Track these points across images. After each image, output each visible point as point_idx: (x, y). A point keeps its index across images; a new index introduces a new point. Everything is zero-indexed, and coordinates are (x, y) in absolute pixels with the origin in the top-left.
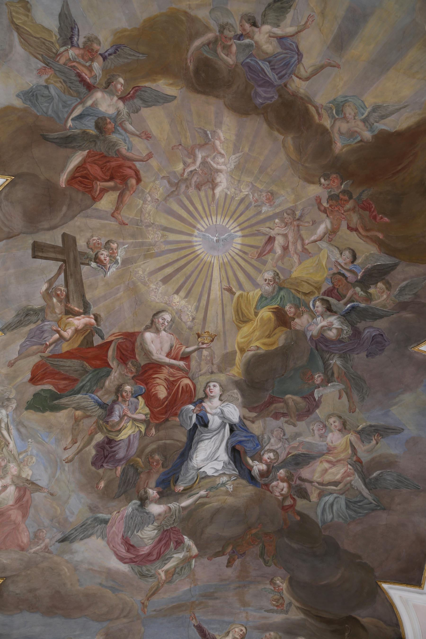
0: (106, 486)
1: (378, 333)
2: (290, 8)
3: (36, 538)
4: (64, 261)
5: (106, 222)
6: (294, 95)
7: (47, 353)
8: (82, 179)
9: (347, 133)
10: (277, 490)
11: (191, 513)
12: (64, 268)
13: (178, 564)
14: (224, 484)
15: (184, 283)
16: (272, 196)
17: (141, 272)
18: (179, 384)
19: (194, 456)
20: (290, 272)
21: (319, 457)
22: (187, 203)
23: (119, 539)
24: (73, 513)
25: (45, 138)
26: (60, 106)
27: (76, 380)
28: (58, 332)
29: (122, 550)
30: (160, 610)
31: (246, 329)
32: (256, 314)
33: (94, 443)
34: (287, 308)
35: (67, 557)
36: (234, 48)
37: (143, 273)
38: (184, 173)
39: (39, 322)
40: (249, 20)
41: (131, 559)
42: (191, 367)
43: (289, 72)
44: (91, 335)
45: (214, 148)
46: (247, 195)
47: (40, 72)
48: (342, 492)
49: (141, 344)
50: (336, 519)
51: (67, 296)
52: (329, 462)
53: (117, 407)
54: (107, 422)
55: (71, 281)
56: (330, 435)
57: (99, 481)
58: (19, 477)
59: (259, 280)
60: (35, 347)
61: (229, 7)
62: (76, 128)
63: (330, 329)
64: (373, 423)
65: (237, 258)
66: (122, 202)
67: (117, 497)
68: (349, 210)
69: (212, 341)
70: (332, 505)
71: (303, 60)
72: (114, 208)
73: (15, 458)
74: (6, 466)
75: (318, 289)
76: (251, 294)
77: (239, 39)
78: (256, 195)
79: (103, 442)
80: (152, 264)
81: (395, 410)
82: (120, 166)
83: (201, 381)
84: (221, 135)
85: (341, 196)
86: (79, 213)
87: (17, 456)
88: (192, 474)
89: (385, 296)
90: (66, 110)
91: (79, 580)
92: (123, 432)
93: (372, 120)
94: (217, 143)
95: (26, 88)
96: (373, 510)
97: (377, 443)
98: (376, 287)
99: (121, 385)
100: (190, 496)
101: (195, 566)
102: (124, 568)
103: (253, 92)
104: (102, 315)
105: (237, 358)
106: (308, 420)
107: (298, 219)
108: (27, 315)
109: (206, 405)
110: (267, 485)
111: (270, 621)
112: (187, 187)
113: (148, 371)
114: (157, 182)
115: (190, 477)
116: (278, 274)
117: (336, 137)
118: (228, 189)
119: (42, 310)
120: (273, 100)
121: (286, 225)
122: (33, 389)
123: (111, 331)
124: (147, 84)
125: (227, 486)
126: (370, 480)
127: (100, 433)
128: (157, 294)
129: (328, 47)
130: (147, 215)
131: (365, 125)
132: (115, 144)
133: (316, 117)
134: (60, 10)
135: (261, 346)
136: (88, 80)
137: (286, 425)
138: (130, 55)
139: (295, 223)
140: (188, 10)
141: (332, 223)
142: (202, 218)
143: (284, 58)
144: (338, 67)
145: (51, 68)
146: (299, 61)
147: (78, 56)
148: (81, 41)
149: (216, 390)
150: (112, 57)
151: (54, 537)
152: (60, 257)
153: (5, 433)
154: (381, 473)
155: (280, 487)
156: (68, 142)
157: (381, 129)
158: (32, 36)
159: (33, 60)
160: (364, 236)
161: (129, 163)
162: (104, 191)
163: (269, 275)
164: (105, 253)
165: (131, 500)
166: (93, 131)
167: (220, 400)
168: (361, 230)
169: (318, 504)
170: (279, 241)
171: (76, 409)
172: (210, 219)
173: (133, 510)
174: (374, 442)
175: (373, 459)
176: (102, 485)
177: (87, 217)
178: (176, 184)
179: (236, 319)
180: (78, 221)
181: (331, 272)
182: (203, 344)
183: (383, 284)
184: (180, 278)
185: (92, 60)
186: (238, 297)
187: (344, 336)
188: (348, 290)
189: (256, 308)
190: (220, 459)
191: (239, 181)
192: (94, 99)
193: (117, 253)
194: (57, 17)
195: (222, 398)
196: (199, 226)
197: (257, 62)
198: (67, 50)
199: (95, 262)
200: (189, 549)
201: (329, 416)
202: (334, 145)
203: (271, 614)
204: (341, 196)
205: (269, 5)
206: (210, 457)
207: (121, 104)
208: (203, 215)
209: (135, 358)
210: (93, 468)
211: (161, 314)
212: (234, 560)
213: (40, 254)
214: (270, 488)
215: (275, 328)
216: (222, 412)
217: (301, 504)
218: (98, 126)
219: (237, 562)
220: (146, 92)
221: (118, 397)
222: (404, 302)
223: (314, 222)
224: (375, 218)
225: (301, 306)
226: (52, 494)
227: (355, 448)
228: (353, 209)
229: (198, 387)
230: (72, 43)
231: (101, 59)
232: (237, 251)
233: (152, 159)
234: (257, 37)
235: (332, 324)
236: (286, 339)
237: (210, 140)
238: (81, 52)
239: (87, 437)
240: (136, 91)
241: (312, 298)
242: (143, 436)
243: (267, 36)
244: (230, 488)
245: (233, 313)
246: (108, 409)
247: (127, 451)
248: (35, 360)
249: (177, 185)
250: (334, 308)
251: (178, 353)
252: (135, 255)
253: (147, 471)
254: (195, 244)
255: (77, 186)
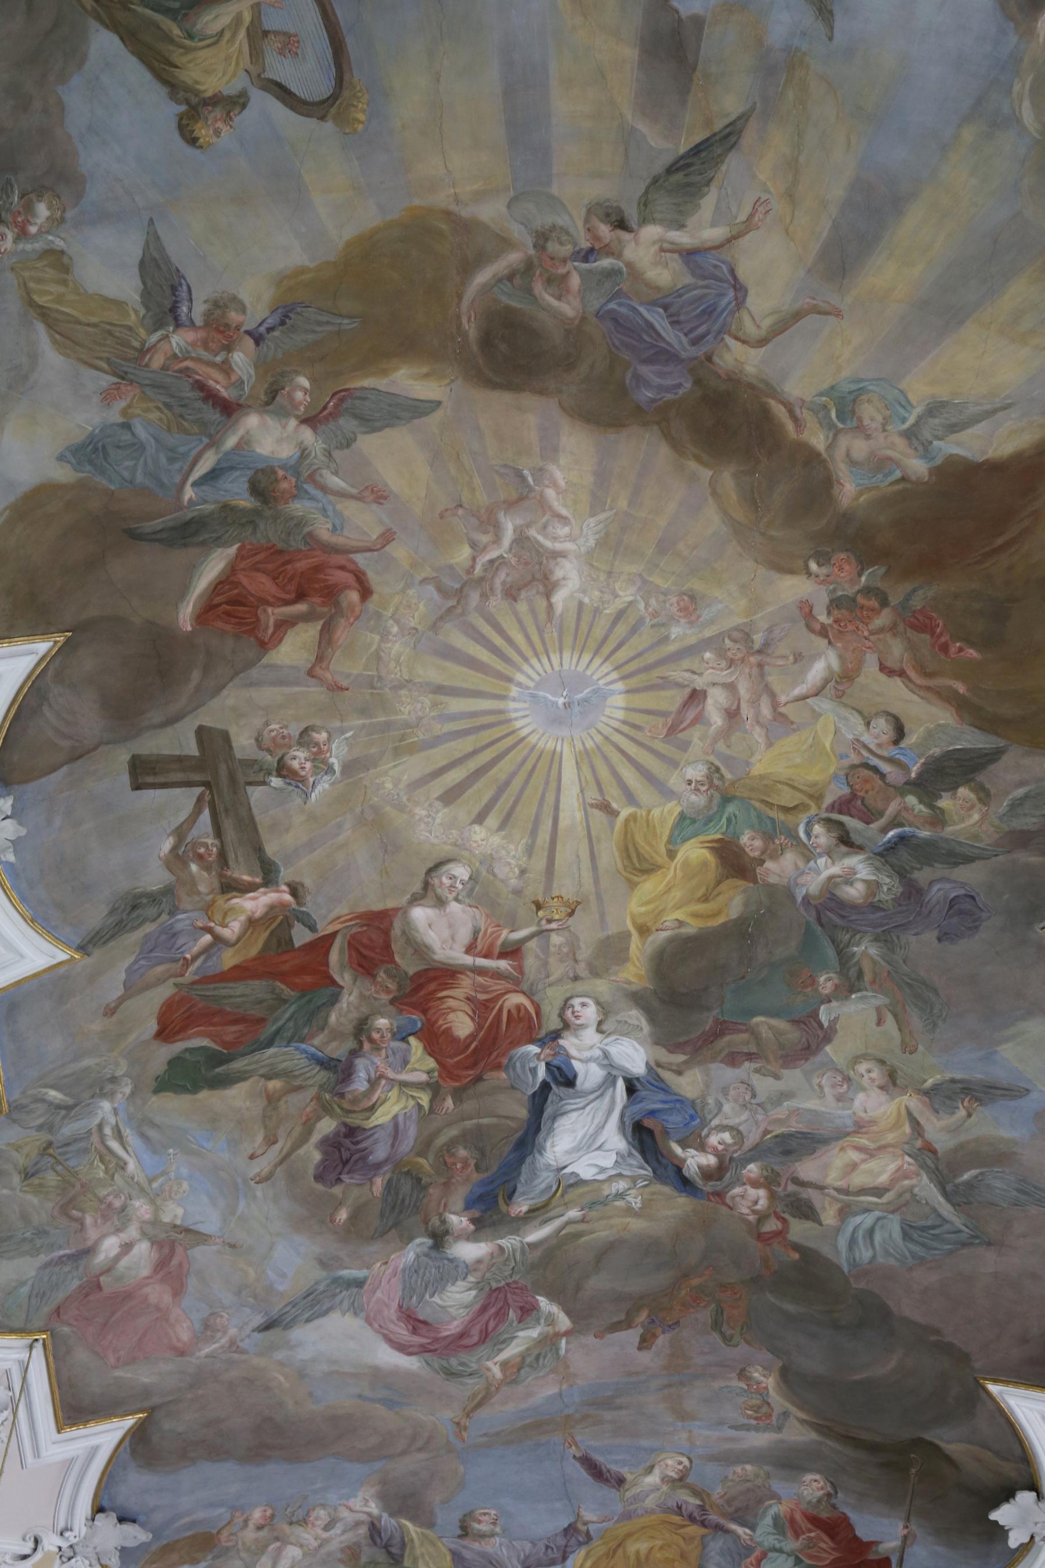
0: (353, 1218)
1: (962, 892)
2: (708, 183)
3: (208, 1328)
4: (206, 784)
5: (296, 689)
6: (730, 379)
7: (190, 975)
8: (232, 608)
9: (868, 462)
10: (744, 1202)
11: (549, 1254)
12: (207, 798)
13: (528, 1349)
14: (620, 1196)
15: (494, 800)
16: (691, 604)
17: (389, 785)
18: (501, 1009)
19: (548, 1144)
20: (748, 764)
21: (838, 1138)
22: (486, 629)
23: (392, 1312)
24: (284, 1275)
25: (135, 536)
26: (163, 460)
27: (261, 1021)
28: (209, 930)
29: (402, 1332)
30: (498, 1434)
31: (649, 886)
32: (672, 854)
33: (316, 1137)
34: (745, 839)
35: (279, 1355)
36: (575, 281)
37: (396, 785)
38: (473, 567)
39: (164, 917)
40: (608, 215)
41: (422, 1346)
42: (527, 970)
43: (716, 327)
44: (287, 924)
45: (543, 505)
46: (631, 603)
47: (108, 397)
48: (895, 1208)
49: (404, 932)
50: (880, 1260)
51: (222, 856)
52: (859, 1149)
53: (361, 1064)
54: (342, 1095)
55: (227, 824)
56: (860, 1097)
57: (336, 1209)
58: (156, 1222)
59: (674, 781)
60: (160, 969)
61: (555, 190)
62: (205, 502)
63: (850, 883)
64: (958, 1076)
65: (617, 738)
66: (330, 642)
67: (381, 1234)
68: (881, 630)
69: (571, 914)
70: (871, 1232)
71: (749, 300)
72: (313, 658)
73: (142, 1190)
74: (123, 1208)
75: (818, 798)
76: (656, 812)
77: (586, 259)
78: (653, 602)
79: (337, 1134)
80: (414, 766)
81: (1007, 1051)
82: (318, 568)
83: (551, 999)
84: (559, 475)
85: (861, 600)
86: (231, 679)
87: (145, 1185)
88: (545, 1179)
89: (976, 817)
90: (177, 466)
91: (311, 1394)
92: (380, 1111)
93: (926, 434)
94: (550, 493)
95: (78, 437)
96: (964, 1245)
97: (969, 1115)
98: (954, 797)
99: (366, 1019)
100: (545, 1222)
101: (567, 1351)
102: (410, 1363)
103: (629, 376)
104: (308, 882)
105: (633, 947)
106: (807, 1066)
107: (759, 652)
108: (133, 907)
109: (568, 1043)
110: (720, 1195)
111: (745, 1445)
112: (484, 596)
113: (425, 986)
114: (411, 592)
115: (543, 1186)
116: (718, 770)
117: (841, 470)
118: (584, 592)
119: (168, 891)
120: (681, 392)
121: (731, 663)
122: (165, 1052)
123: (330, 913)
124: (367, 382)
125: (628, 1198)
126: (956, 1186)
127: (327, 1118)
128: (430, 827)
129: (809, 271)
130: (392, 664)
131: (910, 445)
132: (301, 522)
133: (790, 427)
134: (140, 253)
135: (689, 920)
136: (224, 393)
137: (757, 1076)
138: (319, 323)
139: (753, 660)
140: (453, 208)
141: (841, 657)
142: (526, 660)
143: (700, 299)
144: (838, 314)
145: (131, 382)
146: (740, 302)
147: (193, 344)
148: (199, 310)
149: (590, 1013)
150: (276, 333)
151: (247, 1324)
152: (196, 777)
153: (114, 1145)
154: (981, 1174)
155: (750, 1198)
156: (190, 533)
157: (951, 455)
158: (80, 323)
159: (88, 373)
160: (920, 687)
161: (340, 560)
162: (284, 625)
163: (696, 772)
164: (301, 754)
165: (411, 1239)
166: (245, 501)
167: (599, 1030)
168: (912, 674)
169: (838, 1230)
170: (716, 701)
171: (268, 1077)
172: (545, 660)
173: (418, 1256)
174: (962, 1113)
175: (961, 1146)
176: (343, 1215)
177: (251, 685)
178: (456, 594)
179: (625, 867)
180: (231, 697)
181: (846, 762)
182: (549, 921)
183: (972, 790)
184: (482, 791)
185: (229, 348)
186: (627, 821)
187: (884, 896)
188: (888, 800)
189: (669, 841)
190: (607, 1147)
191: (610, 573)
192: (241, 432)
193: (330, 750)
194: (136, 271)
195: (604, 1027)
196: (519, 677)
197: (634, 310)
198: (166, 337)
199: (279, 775)
200: (551, 1320)
201: (856, 1060)
202: (836, 490)
203: (742, 1434)
204: (861, 600)
205: (655, 180)
206: (585, 1144)
207: (307, 435)
208: (529, 653)
209: (392, 961)
210: (320, 1187)
211: (445, 868)
212: (655, 1336)
213: (150, 779)
214: (728, 1201)
215: (719, 883)
216: (606, 1055)
217: (799, 1230)
218: (256, 489)
219: (662, 1340)
220: (364, 399)
221: (361, 1044)
222: (1022, 832)
223: (798, 657)
224: (945, 648)
225: (777, 835)
226: (233, 1246)
227: (918, 1123)
228: (893, 629)
229: (545, 1008)
230: (176, 319)
231: (249, 342)
232: (616, 724)
233: (393, 543)
234: (630, 253)
235: (853, 871)
236: (746, 904)
237: (531, 490)
238: (201, 334)
239: (298, 1130)
240: (342, 400)
241: (804, 818)
242: (424, 1116)
243: (654, 249)
244: (636, 1203)
245: (617, 854)
246: (341, 1071)
247: (393, 1146)
248: (165, 992)
249: (460, 594)
250: (855, 838)
251: (491, 946)
252: (373, 750)
253: (443, 1180)
254: (514, 715)
255: (219, 624)
